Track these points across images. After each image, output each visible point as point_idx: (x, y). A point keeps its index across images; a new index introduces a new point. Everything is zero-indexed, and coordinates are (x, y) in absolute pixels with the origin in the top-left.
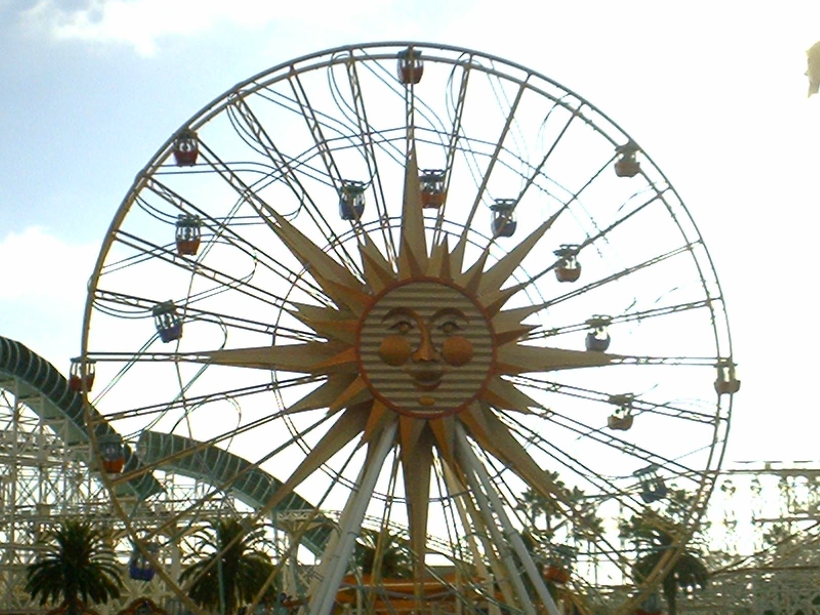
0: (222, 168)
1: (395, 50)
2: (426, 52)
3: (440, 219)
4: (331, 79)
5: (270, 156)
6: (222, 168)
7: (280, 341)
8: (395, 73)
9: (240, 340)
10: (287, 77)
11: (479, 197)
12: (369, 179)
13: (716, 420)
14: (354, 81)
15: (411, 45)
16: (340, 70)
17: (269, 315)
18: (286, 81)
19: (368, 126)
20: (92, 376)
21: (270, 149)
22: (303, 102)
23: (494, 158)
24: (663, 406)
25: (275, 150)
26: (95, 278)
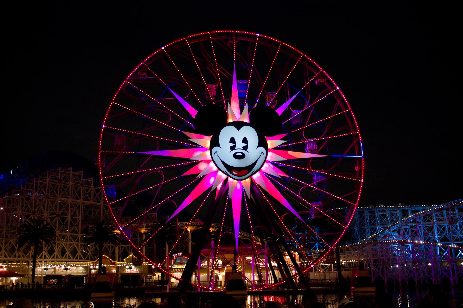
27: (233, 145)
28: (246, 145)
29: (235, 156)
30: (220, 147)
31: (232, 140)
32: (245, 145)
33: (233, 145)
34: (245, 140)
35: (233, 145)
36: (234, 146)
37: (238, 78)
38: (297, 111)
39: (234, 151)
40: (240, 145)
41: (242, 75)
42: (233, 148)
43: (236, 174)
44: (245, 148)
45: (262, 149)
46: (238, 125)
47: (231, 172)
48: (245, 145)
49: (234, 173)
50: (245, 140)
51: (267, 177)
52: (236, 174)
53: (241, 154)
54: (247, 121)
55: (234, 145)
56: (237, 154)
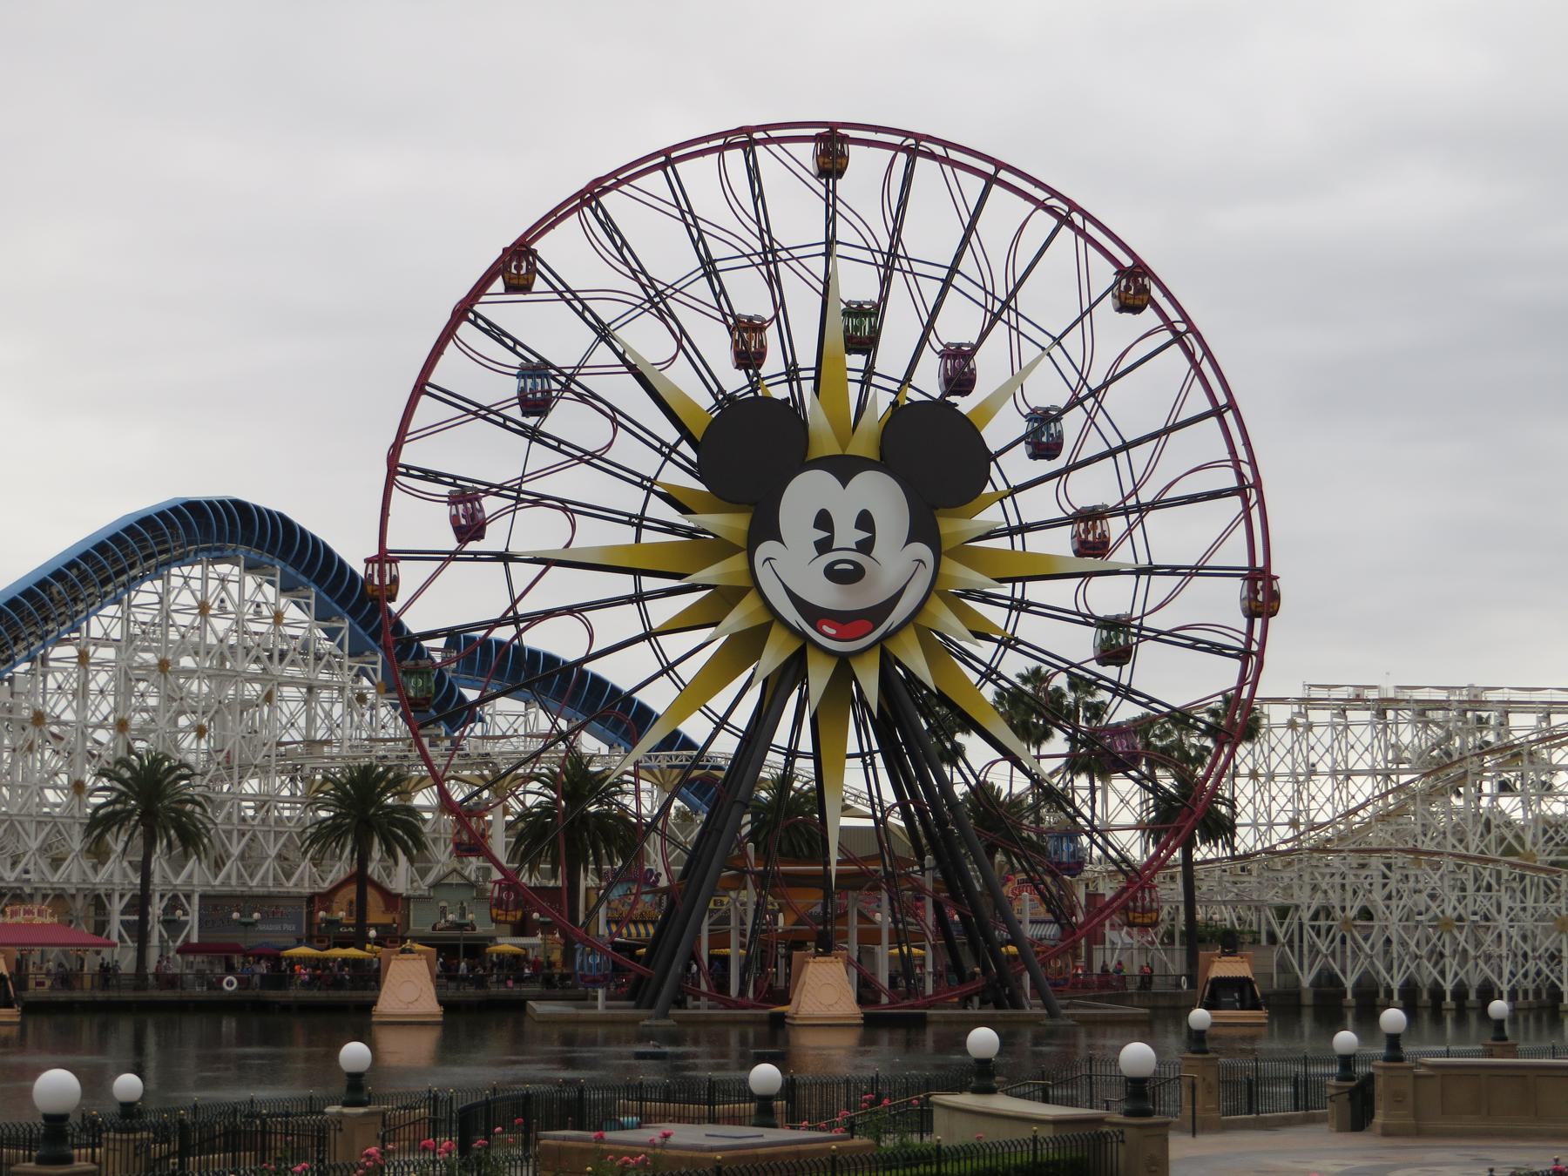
0: (567, 295)
1: (812, 132)
2: (853, 134)
3: (869, 371)
4: (722, 166)
5: (637, 279)
6: (567, 295)
7: (649, 537)
8: (811, 164)
9: (596, 535)
10: (662, 166)
11: (924, 339)
12: (772, 313)
13: (1244, 655)
14: (754, 174)
15: (833, 126)
16: (735, 158)
17: (630, 499)
18: (660, 173)
19: (771, 239)
20: (395, 580)
21: (638, 272)
22: (684, 207)
23: (947, 283)
24: (1169, 633)
25: (644, 272)
26: (396, 448)
27: (824, 534)
28: (867, 535)
29: (831, 573)
30: (782, 542)
31: (824, 520)
32: (865, 535)
34: (865, 521)
35: (824, 534)
36: (830, 540)
39: (829, 558)
40: (847, 534)
42: (823, 546)
43: (833, 632)
44: (865, 547)
45: (922, 550)
46: (844, 468)
47: (818, 626)
48: (865, 535)
49: (826, 628)
50: (865, 521)
52: (833, 632)
53: (851, 567)
54: (871, 453)
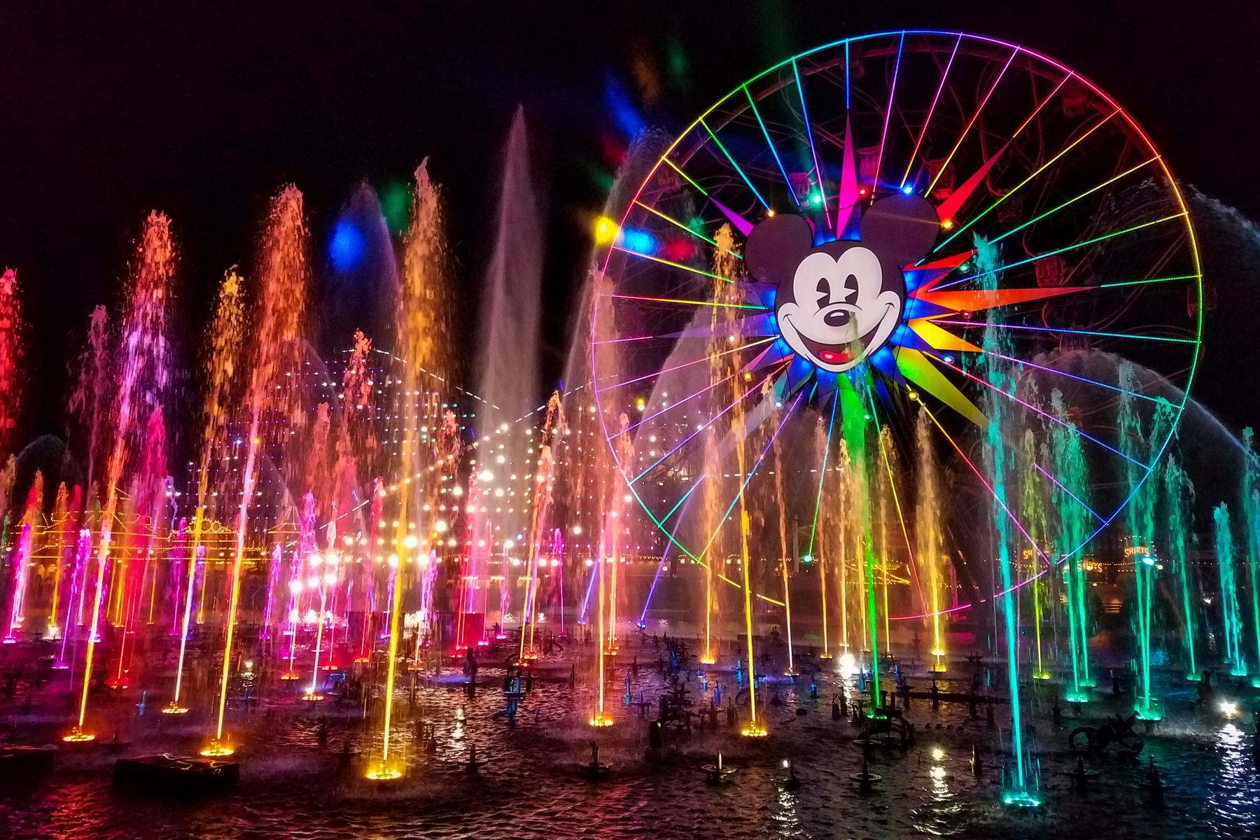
29: (830, 321)
31: (823, 286)
33: (826, 294)
34: (851, 282)
36: (828, 297)
37: (856, 146)
38: (1005, 190)
39: (827, 310)
40: (839, 292)
41: (867, 137)
42: (823, 303)
44: (851, 299)
50: (851, 282)
51: (928, 358)
53: (842, 314)
55: (826, 294)
56: (832, 316)
